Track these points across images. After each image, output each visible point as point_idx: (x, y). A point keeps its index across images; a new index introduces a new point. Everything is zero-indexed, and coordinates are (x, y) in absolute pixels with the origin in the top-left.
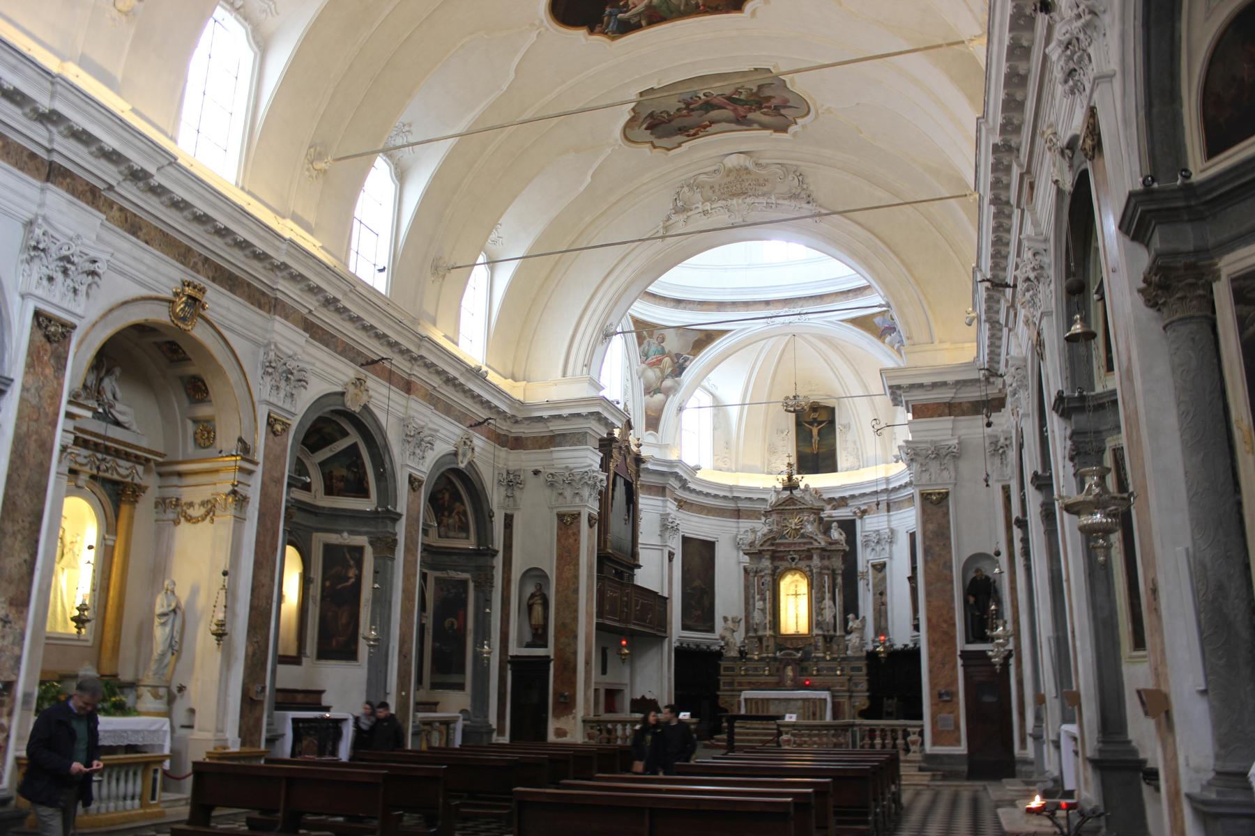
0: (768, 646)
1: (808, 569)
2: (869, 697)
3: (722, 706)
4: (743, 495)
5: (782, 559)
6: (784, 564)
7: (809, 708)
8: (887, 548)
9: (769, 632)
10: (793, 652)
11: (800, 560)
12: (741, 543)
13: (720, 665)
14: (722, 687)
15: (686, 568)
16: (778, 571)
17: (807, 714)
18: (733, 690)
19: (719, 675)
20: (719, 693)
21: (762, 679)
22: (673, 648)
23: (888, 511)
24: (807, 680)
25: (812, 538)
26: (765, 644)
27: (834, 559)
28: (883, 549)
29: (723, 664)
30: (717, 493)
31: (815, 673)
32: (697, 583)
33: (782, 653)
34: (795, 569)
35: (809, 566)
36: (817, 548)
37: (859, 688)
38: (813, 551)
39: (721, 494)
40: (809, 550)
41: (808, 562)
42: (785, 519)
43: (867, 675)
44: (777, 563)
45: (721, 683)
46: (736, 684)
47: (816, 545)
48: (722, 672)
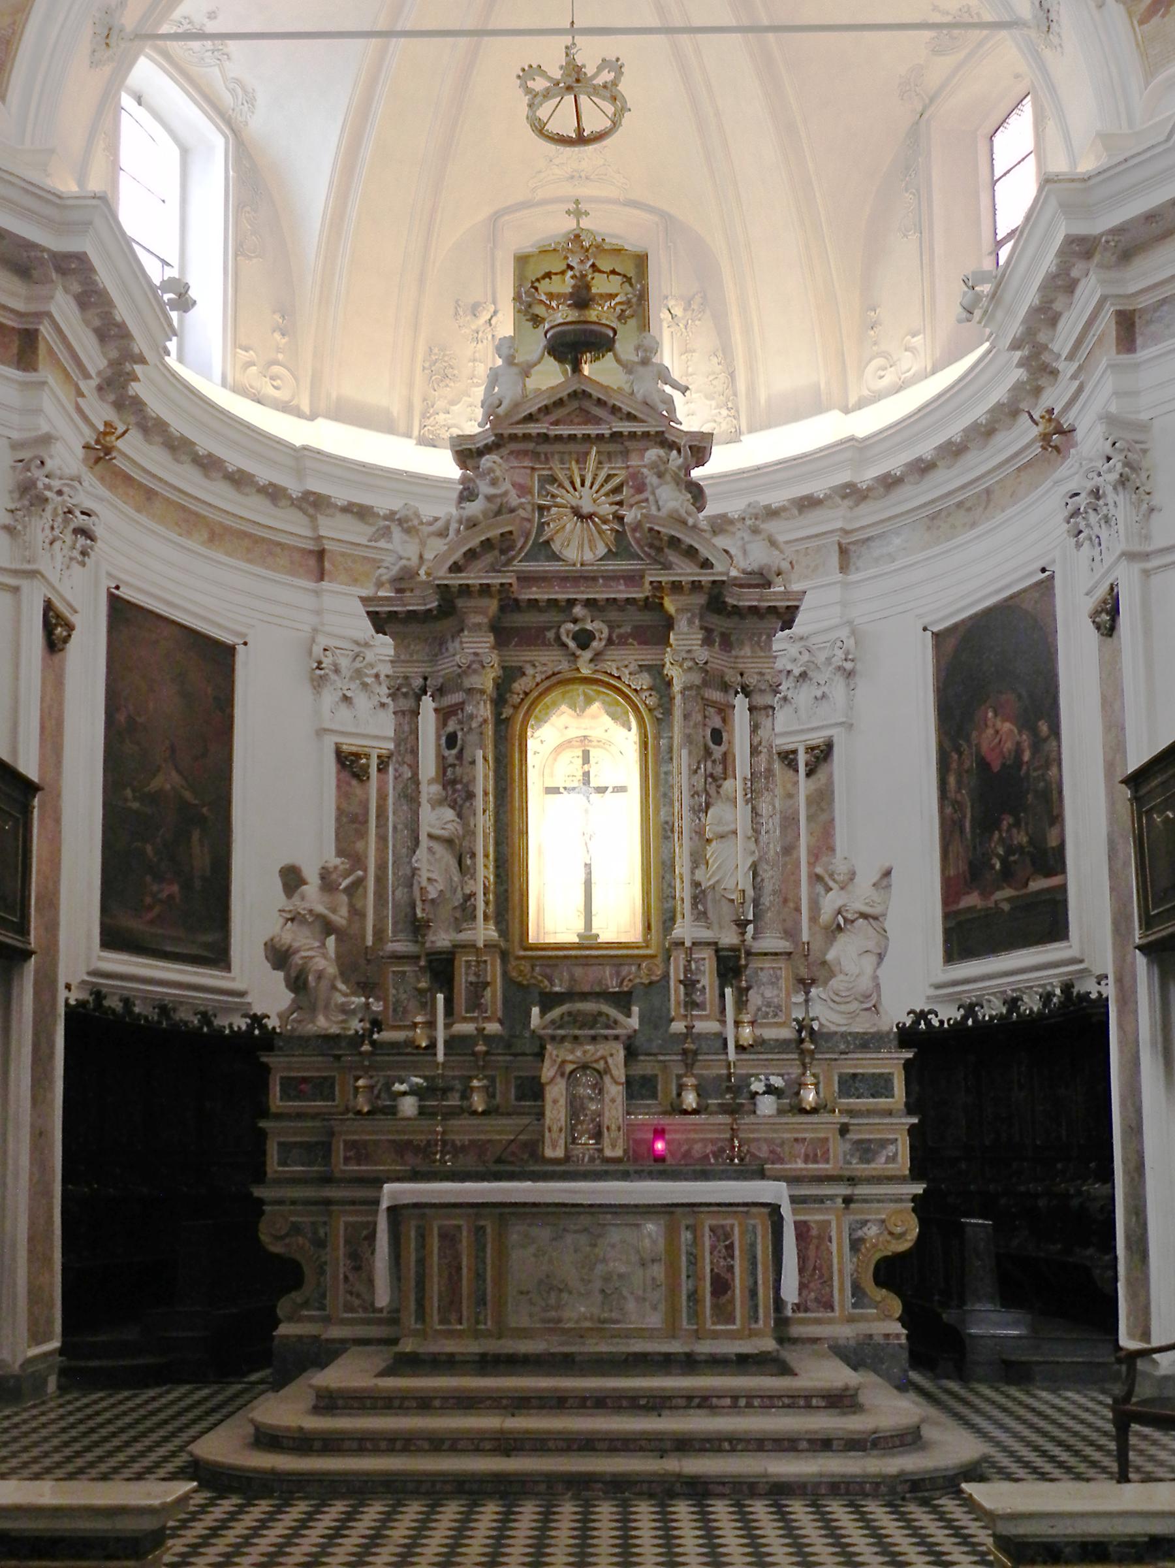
0: (478, 988)
1: (644, 680)
2: (920, 1205)
3: (276, 1248)
4: (341, 494)
5: (534, 638)
6: (546, 660)
7: (693, 1260)
8: (838, 690)
9: (484, 932)
10: (606, 1008)
11: (610, 642)
12: (327, 662)
13: (266, 1069)
14: (273, 1165)
15: (121, 717)
16: (519, 686)
17: (685, 1287)
18: (327, 1180)
19: (265, 1113)
20: (258, 1192)
21: (463, 1130)
22: (61, 1010)
23: (844, 568)
24: (659, 1133)
25: (674, 542)
26: (463, 978)
27: (747, 651)
28: (824, 696)
29: (279, 1065)
30: (250, 466)
31: (690, 1100)
32: (167, 780)
33: (556, 1013)
34: (586, 680)
35: (656, 670)
36: (696, 586)
37: (879, 1165)
38: (670, 605)
39: (264, 474)
40: (652, 605)
41: (647, 655)
42: (553, 480)
43: (910, 1110)
44: (519, 656)
45: (273, 1150)
46: (339, 1150)
47: (686, 571)
48: (276, 1101)
